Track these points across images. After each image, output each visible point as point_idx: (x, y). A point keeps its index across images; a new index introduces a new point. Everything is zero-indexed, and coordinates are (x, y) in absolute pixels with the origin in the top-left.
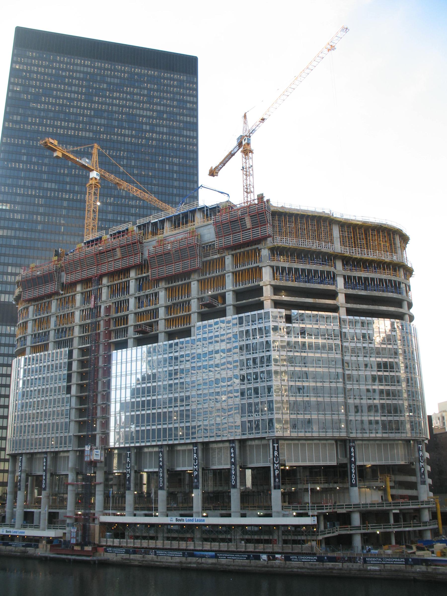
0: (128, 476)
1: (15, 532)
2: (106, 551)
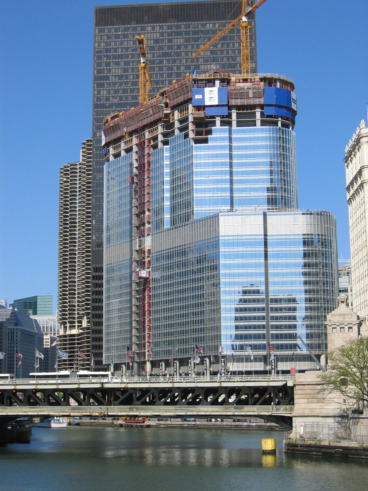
2: (150, 420)
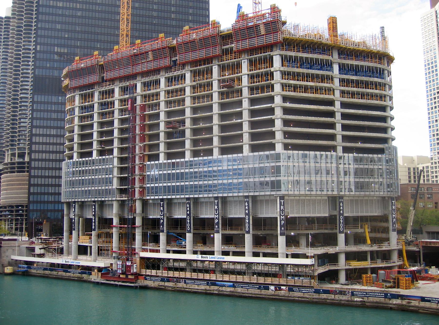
0: (162, 221)
1: (72, 262)
2: (146, 279)
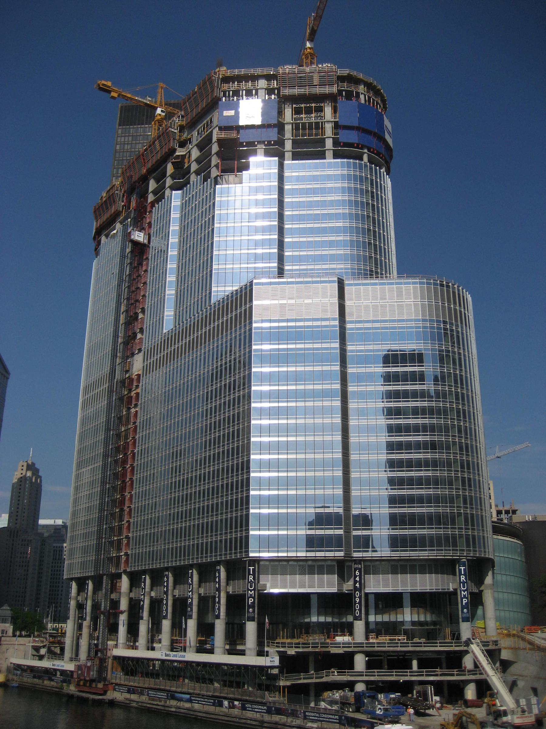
1: (58, 666)
